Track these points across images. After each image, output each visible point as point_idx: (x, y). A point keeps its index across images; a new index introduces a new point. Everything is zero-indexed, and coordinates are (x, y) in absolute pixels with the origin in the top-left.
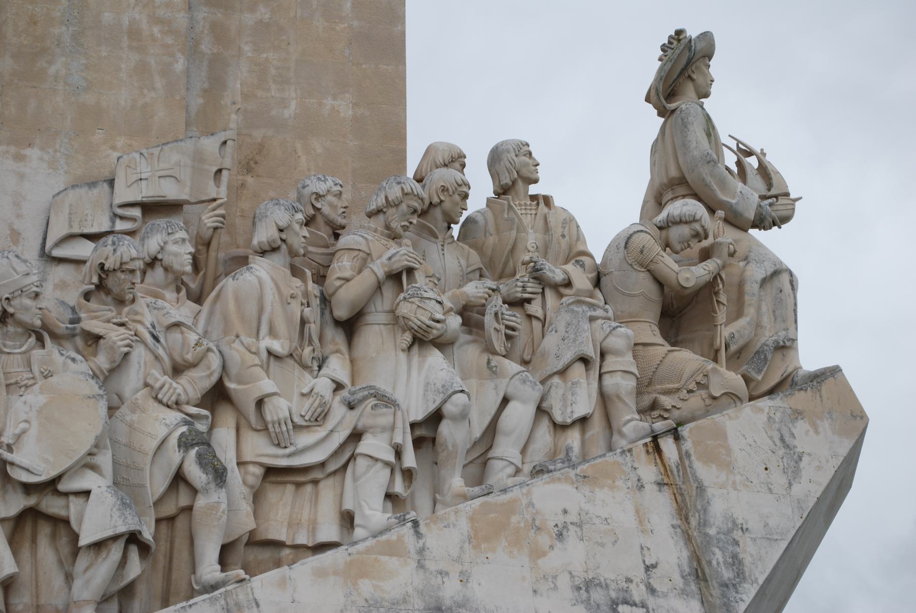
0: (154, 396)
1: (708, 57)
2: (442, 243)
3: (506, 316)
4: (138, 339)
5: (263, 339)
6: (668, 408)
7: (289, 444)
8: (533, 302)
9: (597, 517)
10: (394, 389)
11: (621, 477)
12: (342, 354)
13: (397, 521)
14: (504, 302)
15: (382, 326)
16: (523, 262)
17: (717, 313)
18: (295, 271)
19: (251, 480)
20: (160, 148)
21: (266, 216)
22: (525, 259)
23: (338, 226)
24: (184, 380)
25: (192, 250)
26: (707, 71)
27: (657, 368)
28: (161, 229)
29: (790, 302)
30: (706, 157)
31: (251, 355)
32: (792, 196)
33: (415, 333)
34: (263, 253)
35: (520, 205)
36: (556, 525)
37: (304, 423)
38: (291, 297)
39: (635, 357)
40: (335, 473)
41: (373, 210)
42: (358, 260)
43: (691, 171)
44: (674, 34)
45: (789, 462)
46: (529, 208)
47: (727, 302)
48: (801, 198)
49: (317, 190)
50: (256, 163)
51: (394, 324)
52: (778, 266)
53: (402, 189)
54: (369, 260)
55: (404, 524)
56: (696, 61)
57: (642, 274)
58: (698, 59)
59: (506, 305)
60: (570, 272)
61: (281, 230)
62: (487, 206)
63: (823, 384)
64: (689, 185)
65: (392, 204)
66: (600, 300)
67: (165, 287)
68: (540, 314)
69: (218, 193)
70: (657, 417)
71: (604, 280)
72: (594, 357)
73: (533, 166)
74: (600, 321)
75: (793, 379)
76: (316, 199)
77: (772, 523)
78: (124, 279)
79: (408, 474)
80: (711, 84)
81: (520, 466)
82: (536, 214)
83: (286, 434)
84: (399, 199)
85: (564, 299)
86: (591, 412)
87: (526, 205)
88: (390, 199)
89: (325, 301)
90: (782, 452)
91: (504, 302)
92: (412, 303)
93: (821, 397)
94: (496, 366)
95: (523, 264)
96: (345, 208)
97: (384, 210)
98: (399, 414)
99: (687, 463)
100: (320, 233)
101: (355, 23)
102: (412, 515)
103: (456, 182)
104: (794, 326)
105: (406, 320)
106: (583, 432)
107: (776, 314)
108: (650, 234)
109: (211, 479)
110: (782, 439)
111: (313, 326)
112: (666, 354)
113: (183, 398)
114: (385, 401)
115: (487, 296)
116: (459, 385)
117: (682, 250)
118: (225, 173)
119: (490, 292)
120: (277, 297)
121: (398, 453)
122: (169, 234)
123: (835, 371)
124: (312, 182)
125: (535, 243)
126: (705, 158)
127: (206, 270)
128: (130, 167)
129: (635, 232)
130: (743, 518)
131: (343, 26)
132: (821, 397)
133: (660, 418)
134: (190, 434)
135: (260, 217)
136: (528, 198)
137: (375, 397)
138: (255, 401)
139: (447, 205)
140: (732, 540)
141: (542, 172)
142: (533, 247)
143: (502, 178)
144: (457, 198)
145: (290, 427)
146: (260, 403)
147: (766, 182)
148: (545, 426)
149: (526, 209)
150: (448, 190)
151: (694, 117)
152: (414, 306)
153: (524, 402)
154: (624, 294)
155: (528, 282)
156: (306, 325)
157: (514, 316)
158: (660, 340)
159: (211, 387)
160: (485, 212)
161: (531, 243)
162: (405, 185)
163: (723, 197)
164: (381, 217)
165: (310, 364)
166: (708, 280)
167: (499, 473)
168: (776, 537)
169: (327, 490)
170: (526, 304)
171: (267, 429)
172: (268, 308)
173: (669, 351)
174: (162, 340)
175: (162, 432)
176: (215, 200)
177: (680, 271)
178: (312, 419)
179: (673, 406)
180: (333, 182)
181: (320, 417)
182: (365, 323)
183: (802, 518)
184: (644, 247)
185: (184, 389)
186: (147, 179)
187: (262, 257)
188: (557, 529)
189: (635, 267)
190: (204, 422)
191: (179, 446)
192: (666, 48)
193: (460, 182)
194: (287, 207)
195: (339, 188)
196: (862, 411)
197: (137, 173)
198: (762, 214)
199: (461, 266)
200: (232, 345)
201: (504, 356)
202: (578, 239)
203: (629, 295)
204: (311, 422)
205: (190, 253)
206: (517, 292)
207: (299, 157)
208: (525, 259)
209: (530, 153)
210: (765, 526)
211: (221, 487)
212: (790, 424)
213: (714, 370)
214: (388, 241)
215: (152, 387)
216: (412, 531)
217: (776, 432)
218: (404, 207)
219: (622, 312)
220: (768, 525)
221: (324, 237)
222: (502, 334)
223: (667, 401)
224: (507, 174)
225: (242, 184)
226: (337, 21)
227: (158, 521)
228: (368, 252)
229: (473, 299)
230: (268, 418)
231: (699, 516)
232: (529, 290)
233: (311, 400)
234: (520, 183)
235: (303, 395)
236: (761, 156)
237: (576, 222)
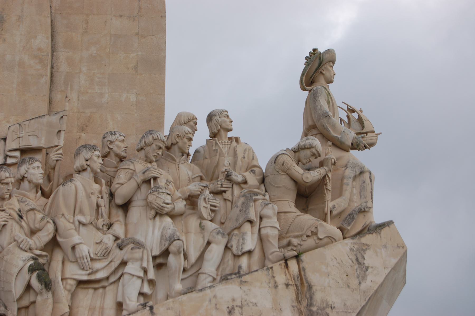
0: (18, 246)
1: (331, 62)
2: (178, 164)
3: (210, 200)
4: (11, 217)
5: (77, 215)
6: (296, 245)
7: (89, 269)
8: (227, 192)
9: (251, 302)
10: (146, 239)
11: (265, 282)
12: (121, 222)
13: (142, 306)
14: (210, 193)
15: (140, 207)
16: (222, 172)
17: (325, 195)
18: (97, 181)
19: (68, 287)
20: (29, 121)
21: (80, 154)
22: (223, 171)
23: (122, 157)
24: (35, 237)
25: (43, 172)
26: (331, 70)
27: (291, 224)
28: (26, 162)
29: (369, 188)
30: (325, 114)
31: (69, 224)
32: (376, 132)
33: (156, 210)
34: (79, 172)
35: (222, 143)
36: (228, 307)
37: (97, 258)
38: (91, 194)
39: (278, 219)
40: (114, 282)
41: (139, 148)
42: (128, 173)
43: (317, 122)
44: (312, 51)
45: (360, 272)
46: (227, 144)
47: (332, 188)
48: (381, 133)
49: (110, 139)
50: (87, 126)
51: (147, 206)
52: (363, 169)
53: (153, 137)
54: (135, 174)
55: (145, 308)
56: (324, 64)
57: (284, 176)
58: (325, 63)
59: (212, 194)
60: (246, 176)
61: (87, 160)
62: (207, 144)
63: (382, 230)
64: (318, 129)
65: (148, 144)
66: (262, 191)
67: (30, 191)
68: (230, 198)
69: (59, 142)
70: (291, 250)
71: (266, 180)
72: (255, 220)
73: (229, 122)
74: (261, 201)
75: (369, 228)
76: (110, 143)
77: (348, 303)
78: (3, 188)
79: (151, 282)
80: (334, 76)
81: (215, 277)
82: (230, 147)
83: (87, 264)
84: (151, 142)
85: (243, 190)
86: (253, 249)
87: (225, 142)
88: (147, 142)
89: (112, 195)
90: (356, 267)
91: (210, 193)
92: (154, 195)
93: (381, 237)
94: (204, 226)
95: (222, 173)
96: (126, 147)
97: (144, 148)
98: (145, 251)
99: (303, 273)
100: (112, 161)
101: (140, 53)
102: (150, 303)
103: (185, 132)
104: (370, 200)
105: (151, 204)
106: (250, 258)
107: (361, 194)
108: (288, 155)
109: (43, 287)
110: (357, 260)
111: (103, 208)
112: (296, 217)
113: (33, 246)
114: (139, 245)
115: (201, 190)
116: (177, 236)
117: (307, 163)
118: (63, 133)
119: (203, 188)
120: (84, 194)
121: (145, 271)
122: (30, 164)
123: (388, 224)
124: (108, 135)
125: (229, 162)
126: (324, 115)
127: (53, 181)
128: (14, 131)
129: (280, 155)
130: (332, 302)
131: (133, 55)
132: (381, 237)
133: (292, 250)
134: (34, 265)
135: (77, 154)
136: (227, 139)
137: (133, 243)
138: (71, 247)
139: (180, 144)
140: (325, 313)
141: (234, 126)
142: (227, 164)
143: (213, 129)
144: (185, 140)
145: (89, 260)
146: (73, 248)
147: (361, 125)
148: (229, 256)
149: (225, 144)
150: (180, 136)
151: (320, 93)
152: (155, 197)
153: (217, 244)
154: (274, 186)
155: (224, 182)
156: (100, 208)
157: (215, 200)
158: (294, 209)
159: (49, 241)
160: (204, 147)
161: (226, 162)
162: (155, 135)
163: (333, 134)
164: (143, 151)
165: (101, 227)
166: (319, 178)
167: (204, 281)
168: (350, 311)
169: (110, 290)
170: (223, 193)
171: (77, 261)
172: (79, 200)
173: (298, 215)
174: (24, 218)
175: (21, 264)
176: (57, 146)
177: (304, 174)
178: (101, 255)
179: (298, 244)
180: (119, 134)
181: (107, 253)
182: (132, 206)
183: (365, 300)
184: (284, 162)
185: (35, 242)
186: (22, 137)
187: (79, 174)
188: (228, 309)
189: (280, 172)
190: (45, 258)
191: (29, 271)
192: (308, 59)
193: (187, 132)
194: (90, 149)
195: (123, 138)
196: (403, 243)
197: (18, 134)
198: (357, 142)
199: (188, 175)
200: (60, 219)
201: (211, 221)
202: (253, 159)
203: (277, 187)
204: (101, 257)
205: (41, 173)
206: (218, 187)
207: (109, 122)
208: (223, 171)
209: (228, 116)
210: (344, 305)
211: (49, 291)
212: (363, 251)
213: (321, 225)
214: (146, 164)
215: (17, 241)
216: (149, 311)
217: (354, 256)
218: (154, 146)
219: (274, 196)
220: (346, 304)
221: (115, 163)
222: (208, 209)
223: (295, 241)
224: (215, 127)
225: (79, 137)
226: (131, 53)
227: (19, 309)
228: (134, 170)
229: (193, 192)
230: (78, 256)
231: (308, 301)
232: (224, 186)
233: (101, 246)
234: (222, 132)
235: (97, 243)
236: (360, 113)
237: (253, 150)
